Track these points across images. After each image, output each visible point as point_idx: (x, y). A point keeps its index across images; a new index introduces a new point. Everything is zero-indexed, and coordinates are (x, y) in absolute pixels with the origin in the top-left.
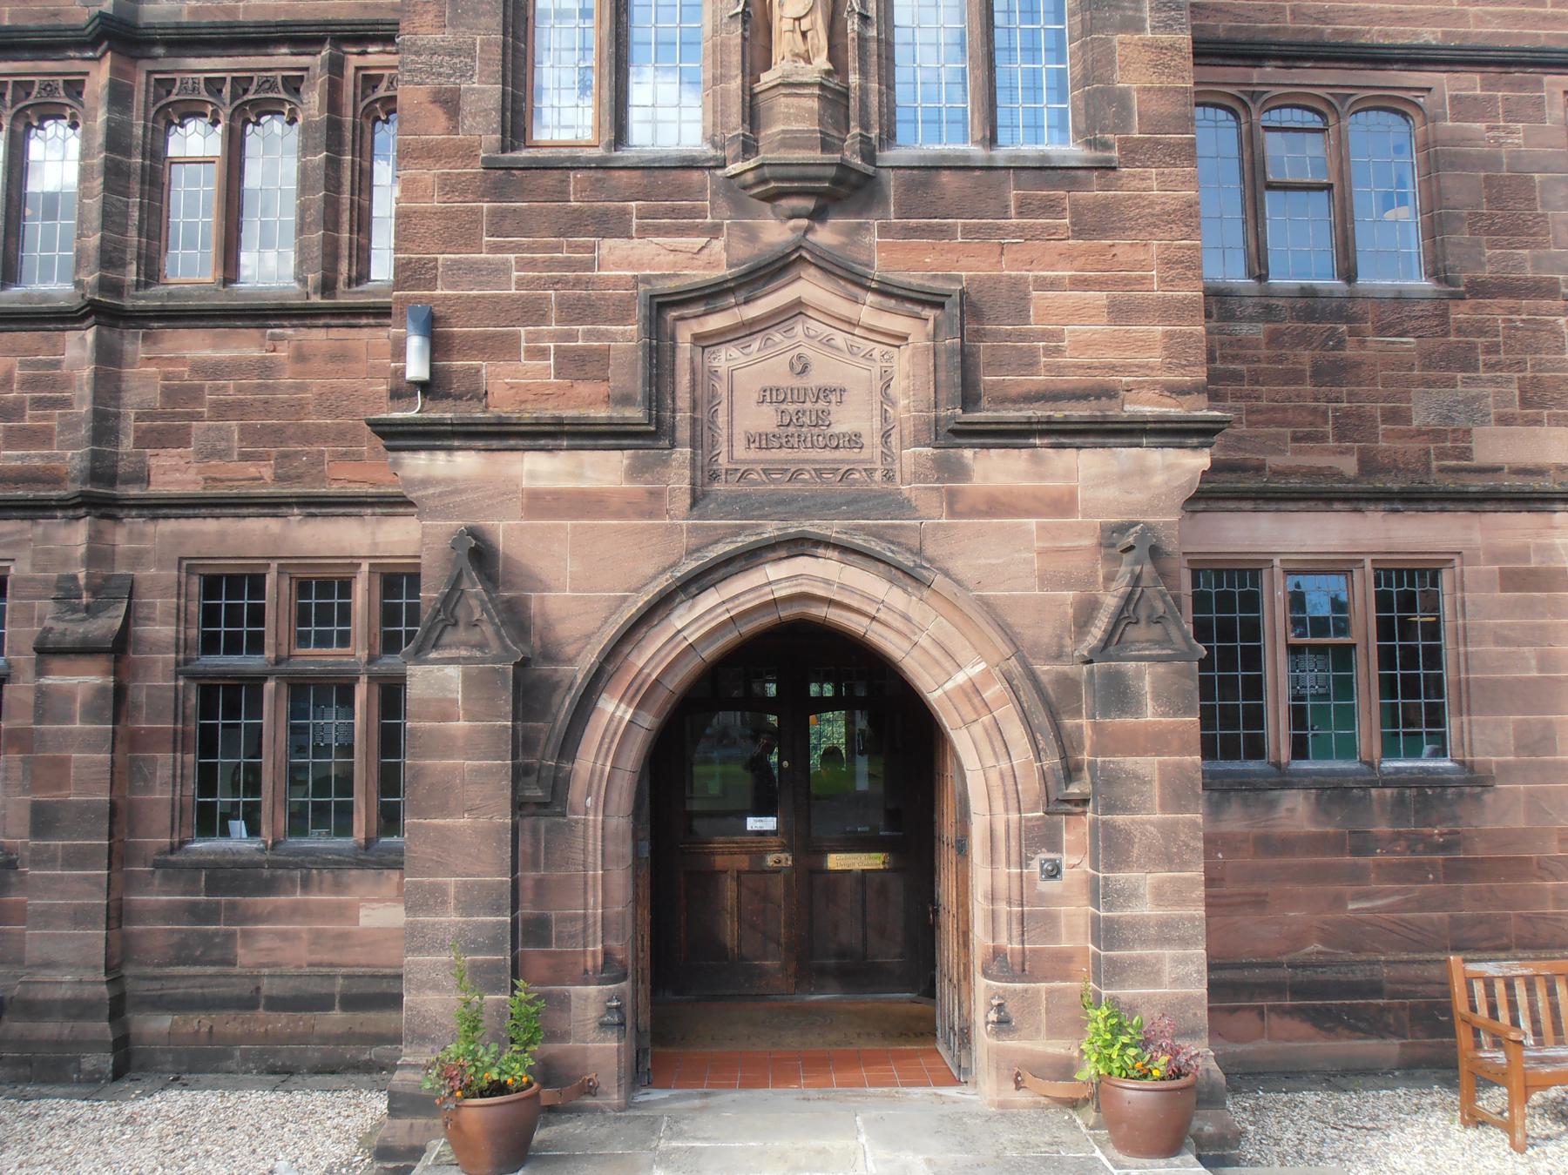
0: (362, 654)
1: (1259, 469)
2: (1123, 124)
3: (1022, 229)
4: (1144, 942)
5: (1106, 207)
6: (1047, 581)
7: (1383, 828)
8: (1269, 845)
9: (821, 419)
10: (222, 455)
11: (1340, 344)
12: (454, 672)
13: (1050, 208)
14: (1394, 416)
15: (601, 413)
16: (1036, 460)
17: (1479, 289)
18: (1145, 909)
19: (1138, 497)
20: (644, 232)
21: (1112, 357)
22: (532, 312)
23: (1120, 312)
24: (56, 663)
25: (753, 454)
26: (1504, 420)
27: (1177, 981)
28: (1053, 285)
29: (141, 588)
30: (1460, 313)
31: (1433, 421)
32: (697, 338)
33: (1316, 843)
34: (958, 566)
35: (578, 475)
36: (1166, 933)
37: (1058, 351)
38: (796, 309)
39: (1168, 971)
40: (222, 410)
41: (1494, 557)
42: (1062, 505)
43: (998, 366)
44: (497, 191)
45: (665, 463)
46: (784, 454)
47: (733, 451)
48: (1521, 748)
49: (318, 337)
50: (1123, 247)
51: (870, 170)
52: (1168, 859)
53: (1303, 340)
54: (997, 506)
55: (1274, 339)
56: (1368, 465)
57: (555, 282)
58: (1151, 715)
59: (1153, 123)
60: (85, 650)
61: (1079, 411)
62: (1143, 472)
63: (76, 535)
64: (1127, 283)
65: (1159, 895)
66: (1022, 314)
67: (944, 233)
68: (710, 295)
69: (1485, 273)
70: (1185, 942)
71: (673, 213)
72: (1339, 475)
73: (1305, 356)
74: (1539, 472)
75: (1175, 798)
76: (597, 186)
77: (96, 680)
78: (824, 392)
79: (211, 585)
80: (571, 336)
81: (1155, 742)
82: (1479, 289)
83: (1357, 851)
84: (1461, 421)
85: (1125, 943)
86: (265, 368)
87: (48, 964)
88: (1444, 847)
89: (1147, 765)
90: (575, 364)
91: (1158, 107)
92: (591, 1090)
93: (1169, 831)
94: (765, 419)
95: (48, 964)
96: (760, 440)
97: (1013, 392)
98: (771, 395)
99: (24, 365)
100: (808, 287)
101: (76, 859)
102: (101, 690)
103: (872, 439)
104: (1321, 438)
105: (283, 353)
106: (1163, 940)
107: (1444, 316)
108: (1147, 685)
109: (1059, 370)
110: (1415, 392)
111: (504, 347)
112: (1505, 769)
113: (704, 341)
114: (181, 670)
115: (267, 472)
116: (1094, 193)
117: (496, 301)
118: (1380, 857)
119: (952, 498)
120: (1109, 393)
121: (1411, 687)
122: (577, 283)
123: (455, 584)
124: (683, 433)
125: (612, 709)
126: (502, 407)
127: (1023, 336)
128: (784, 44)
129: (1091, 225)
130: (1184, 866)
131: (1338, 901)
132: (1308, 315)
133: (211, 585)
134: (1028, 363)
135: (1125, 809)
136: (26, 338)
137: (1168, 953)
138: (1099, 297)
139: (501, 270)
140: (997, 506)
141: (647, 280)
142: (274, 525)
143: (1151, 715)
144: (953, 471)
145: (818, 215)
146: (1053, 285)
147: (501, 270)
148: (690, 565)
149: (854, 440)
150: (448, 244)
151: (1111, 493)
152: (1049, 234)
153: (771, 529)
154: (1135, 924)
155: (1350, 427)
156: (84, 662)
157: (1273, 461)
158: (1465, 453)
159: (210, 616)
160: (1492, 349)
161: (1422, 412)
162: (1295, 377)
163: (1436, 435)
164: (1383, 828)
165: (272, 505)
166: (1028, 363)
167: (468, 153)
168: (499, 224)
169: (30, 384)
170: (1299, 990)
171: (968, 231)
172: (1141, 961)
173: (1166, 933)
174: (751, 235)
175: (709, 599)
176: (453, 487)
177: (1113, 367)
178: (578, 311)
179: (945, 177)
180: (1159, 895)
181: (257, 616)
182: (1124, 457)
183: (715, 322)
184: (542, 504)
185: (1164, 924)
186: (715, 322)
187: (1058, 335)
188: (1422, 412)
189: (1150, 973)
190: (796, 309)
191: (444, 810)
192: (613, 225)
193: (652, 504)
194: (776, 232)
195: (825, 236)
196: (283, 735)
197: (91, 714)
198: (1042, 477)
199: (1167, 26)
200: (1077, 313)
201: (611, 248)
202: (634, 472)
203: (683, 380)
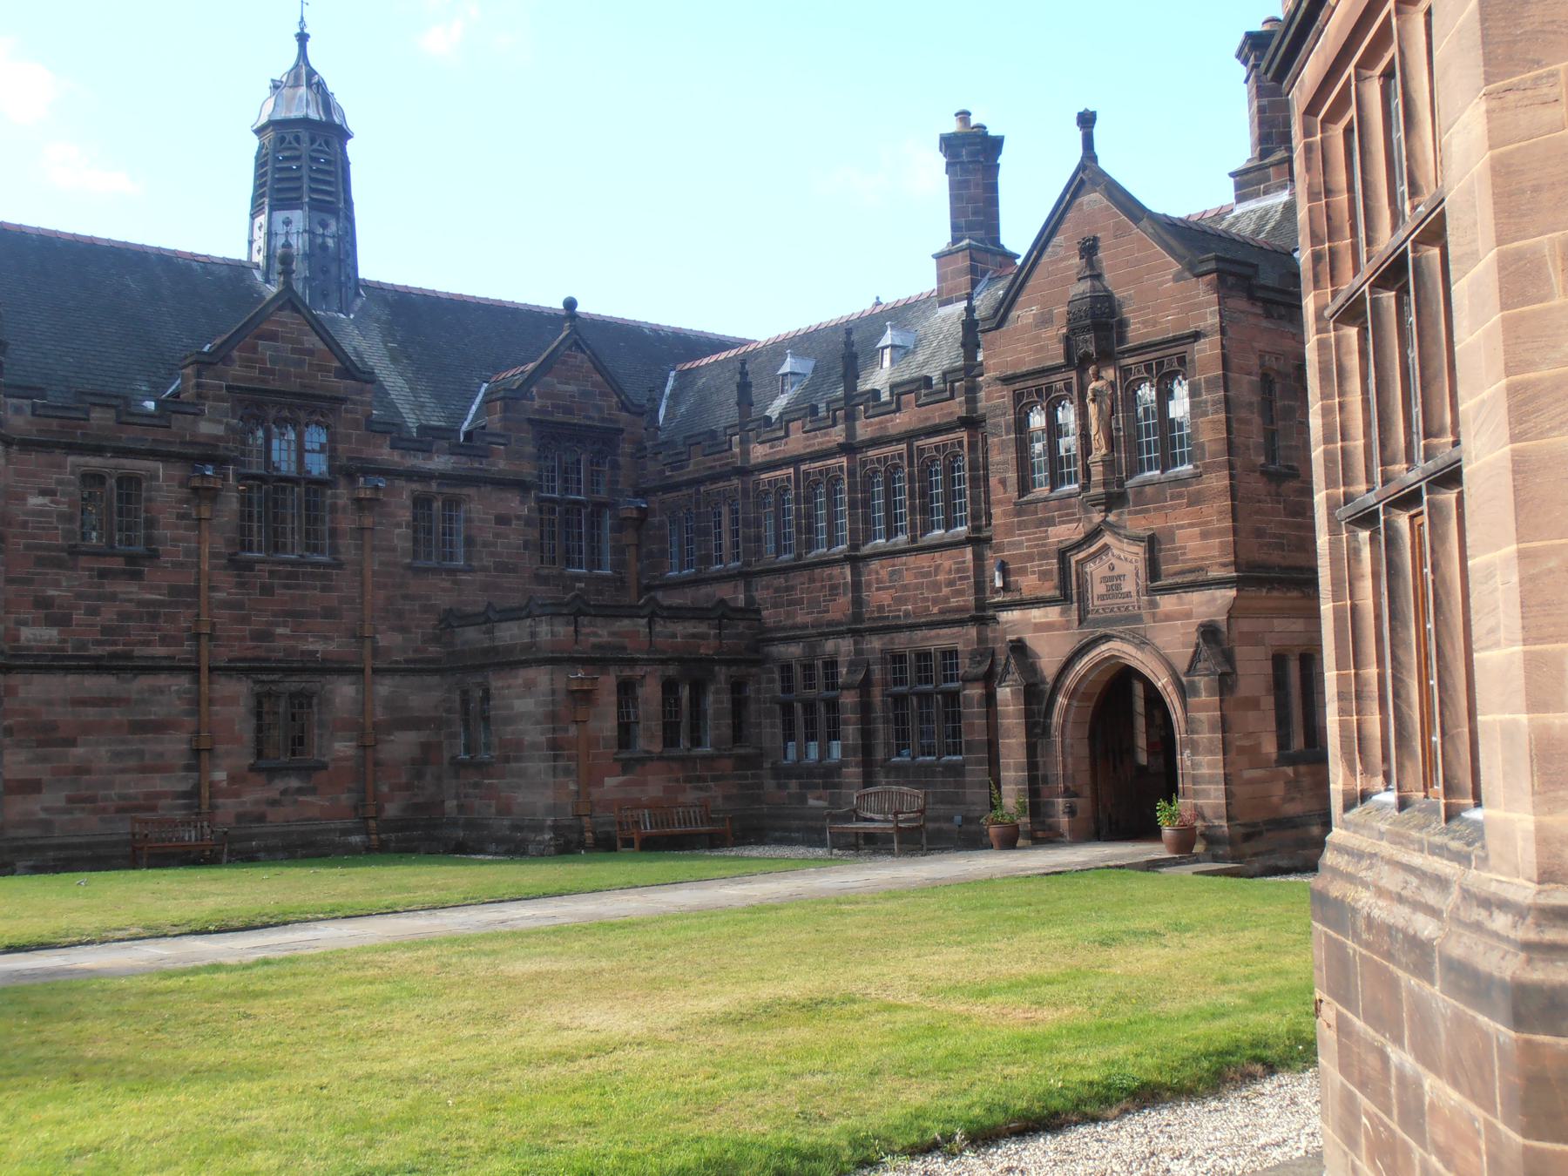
3: (1171, 506)
4: (1204, 783)
5: (1199, 492)
9: (1118, 587)
12: (1008, 689)
13: (1180, 496)
16: (1179, 598)
18: (1205, 771)
19: (1212, 610)
21: (1202, 554)
22: (1030, 557)
23: (1205, 535)
24: (968, 685)
25: (1100, 603)
27: (1216, 798)
28: (1182, 527)
29: (998, 651)
32: (1077, 562)
35: (1046, 616)
36: (1211, 780)
37: (1184, 554)
38: (1106, 548)
39: (1213, 794)
42: (1188, 615)
43: (1167, 563)
44: (1018, 514)
45: (1070, 609)
46: (1109, 602)
47: (1094, 603)
51: (1122, 490)
52: (1211, 752)
57: (1037, 545)
58: (1204, 697)
59: (1214, 455)
60: (975, 679)
61: (1189, 578)
62: (1214, 599)
63: (972, 631)
64: (1206, 523)
66: (1173, 541)
67: (1147, 511)
68: (1078, 546)
70: (1217, 783)
71: (1067, 515)
75: (1212, 730)
76: (1046, 509)
77: (979, 691)
78: (1119, 577)
80: (1041, 565)
81: (1204, 707)
85: (1199, 783)
87: (974, 804)
89: (1202, 716)
90: (1044, 575)
91: (1214, 447)
92: (1062, 835)
93: (1211, 740)
95: (974, 804)
96: (1101, 597)
97: (1171, 572)
98: (1104, 579)
99: (955, 563)
100: (1107, 538)
101: (979, 762)
102: (982, 695)
103: (1134, 594)
106: (1210, 783)
108: (1202, 685)
109: (1184, 561)
113: (1080, 563)
117: (1020, 555)
119: (1154, 615)
122: (1043, 545)
123: (1007, 658)
124: (1075, 598)
125: (1061, 700)
126: (1026, 595)
127: (1174, 549)
128: (1094, 445)
129: (1195, 500)
130: (1215, 754)
135: (1197, 733)
136: (954, 552)
137: (1212, 787)
138: (1197, 530)
139: (1021, 543)
140: (1168, 617)
141: (1061, 542)
143: (1204, 697)
144: (1153, 604)
145: (1108, 510)
146: (1182, 527)
149: (1128, 595)
151: (1203, 609)
152: (1180, 505)
154: (1202, 776)
156: (976, 684)
166: (1176, 561)
167: (1009, 501)
168: (1021, 525)
169: (958, 570)
171: (1155, 509)
172: (1204, 790)
173: (1211, 780)
174: (1090, 520)
177: (1203, 559)
179: (1147, 488)
182: (1205, 595)
183: (1082, 555)
185: (1211, 776)
186: (1082, 555)
187: (1185, 548)
189: (1206, 794)
190: (1106, 548)
191: (1008, 737)
192: (1050, 522)
193: (1066, 626)
194: (1097, 518)
195: (1111, 518)
197: (980, 706)
198: (1181, 604)
199: (1216, 412)
200: (1191, 538)
202: (1063, 613)
203: (1074, 578)
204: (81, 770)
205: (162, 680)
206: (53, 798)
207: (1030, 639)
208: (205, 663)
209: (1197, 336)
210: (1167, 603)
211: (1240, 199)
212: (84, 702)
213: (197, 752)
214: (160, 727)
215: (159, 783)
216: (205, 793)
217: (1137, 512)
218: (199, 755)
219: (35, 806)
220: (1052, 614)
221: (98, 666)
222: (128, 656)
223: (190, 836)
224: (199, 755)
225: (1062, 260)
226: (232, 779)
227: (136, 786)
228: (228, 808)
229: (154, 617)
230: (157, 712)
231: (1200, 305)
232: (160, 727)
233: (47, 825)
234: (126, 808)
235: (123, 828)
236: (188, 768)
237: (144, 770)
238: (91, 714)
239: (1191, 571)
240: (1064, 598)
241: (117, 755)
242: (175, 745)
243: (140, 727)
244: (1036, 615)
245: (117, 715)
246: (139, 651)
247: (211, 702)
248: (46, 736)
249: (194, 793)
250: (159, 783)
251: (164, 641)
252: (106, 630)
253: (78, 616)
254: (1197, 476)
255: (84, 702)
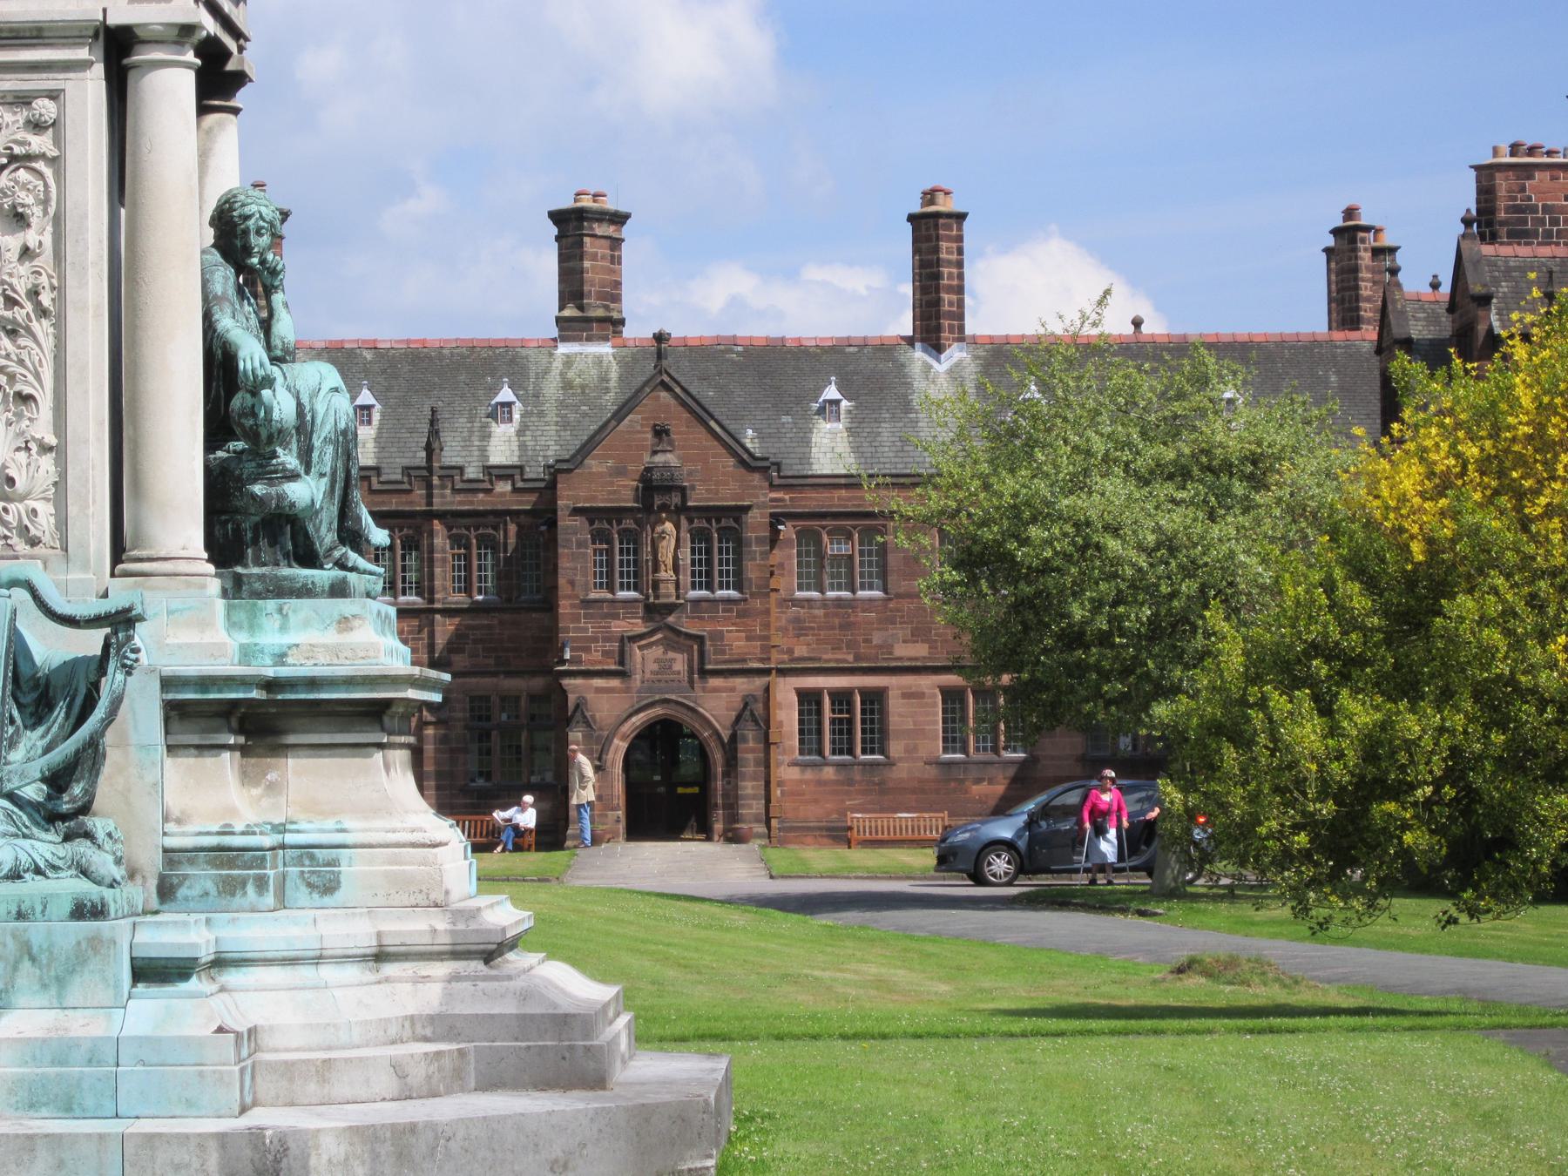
0: (525, 722)
1: (819, 659)
2: (750, 588)
5: (745, 611)
6: (727, 709)
7: (858, 777)
8: (820, 783)
9: (670, 667)
10: (477, 656)
11: (849, 616)
14: (866, 641)
15: (613, 667)
17: (899, 596)
19: (752, 687)
20: (624, 618)
21: (746, 650)
22: (595, 640)
23: (748, 639)
26: (904, 641)
28: (731, 631)
30: (891, 605)
31: (880, 642)
33: (837, 782)
34: (706, 706)
36: (754, 797)
40: (475, 641)
41: (899, 688)
42: (733, 690)
48: (907, 751)
49: (506, 617)
50: (748, 621)
52: (755, 779)
53: (836, 615)
54: (716, 690)
55: (826, 615)
56: (857, 658)
58: (751, 744)
65: (753, 788)
69: (902, 590)
72: (845, 661)
73: (837, 621)
74: (916, 659)
79: (472, 699)
81: (753, 751)
82: (899, 596)
83: (849, 785)
84: (890, 641)
86: (489, 627)
88: (878, 784)
89: (750, 756)
90: (606, 654)
93: (755, 772)
94: (655, 667)
104: (840, 648)
105: (495, 622)
107: (886, 606)
110: (874, 633)
111: (587, 650)
112: (900, 759)
114: (466, 727)
115: (491, 661)
116: (742, 606)
118: (857, 787)
120: (744, 661)
121: (954, 720)
131: (843, 801)
132: (839, 606)
133: (472, 699)
134: (723, 652)
140: (716, 690)
142: (495, 680)
143: (751, 744)
147: (586, 630)
148: (637, 706)
149: (679, 673)
150: (572, 622)
151: (745, 686)
153: (657, 697)
155: (851, 645)
157: (825, 657)
158: (891, 653)
159: (472, 710)
160: (902, 617)
161: (877, 638)
162: (832, 628)
163: (880, 647)
164: (858, 777)
165: (494, 674)
166: (723, 652)
170: (828, 829)
175: (642, 715)
176: (577, 686)
178: (606, 639)
180: (753, 788)
181: (488, 709)
183: (643, 642)
184: (599, 690)
188: (877, 638)
189: (750, 807)
192: (616, 617)
193: (627, 690)
196: (498, 748)
200: (738, 639)
201: (614, 623)
207: (590, 696)
209: (749, 508)
210: (715, 682)
211: (564, 339)
217: (693, 618)
220: (615, 683)
225: (639, 432)
231: (755, 487)
239: (737, 661)
240: (622, 674)
244: (598, 682)
254: (745, 600)
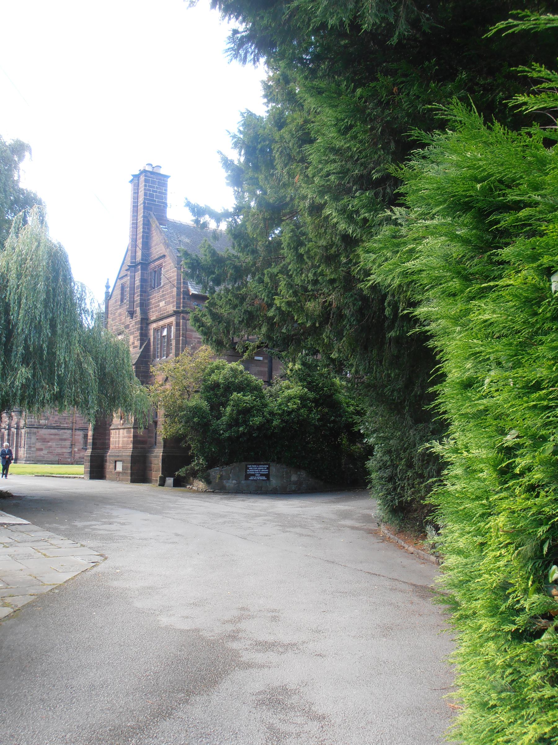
204: (50, 447)
205: (66, 431)
206: (45, 452)
208: (74, 428)
212: (51, 435)
213: (72, 445)
214: (65, 440)
215: (64, 450)
216: (73, 452)
218: (72, 445)
219: (41, 453)
221: (54, 428)
222: (60, 426)
223: (69, 460)
224: (72, 445)
226: (78, 450)
227: (59, 451)
228: (77, 456)
229: (65, 419)
230: (64, 437)
232: (65, 440)
233: (43, 457)
234: (58, 455)
235: (57, 459)
236: (70, 448)
237: (62, 448)
238: (52, 437)
241: (57, 445)
242: (68, 443)
243: (61, 440)
245: (57, 437)
246: (62, 425)
247: (75, 435)
248: (44, 440)
249: (71, 452)
250: (64, 450)
251: (67, 423)
252: (56, 421)
253: (51, 419)
255: (51, 435)
